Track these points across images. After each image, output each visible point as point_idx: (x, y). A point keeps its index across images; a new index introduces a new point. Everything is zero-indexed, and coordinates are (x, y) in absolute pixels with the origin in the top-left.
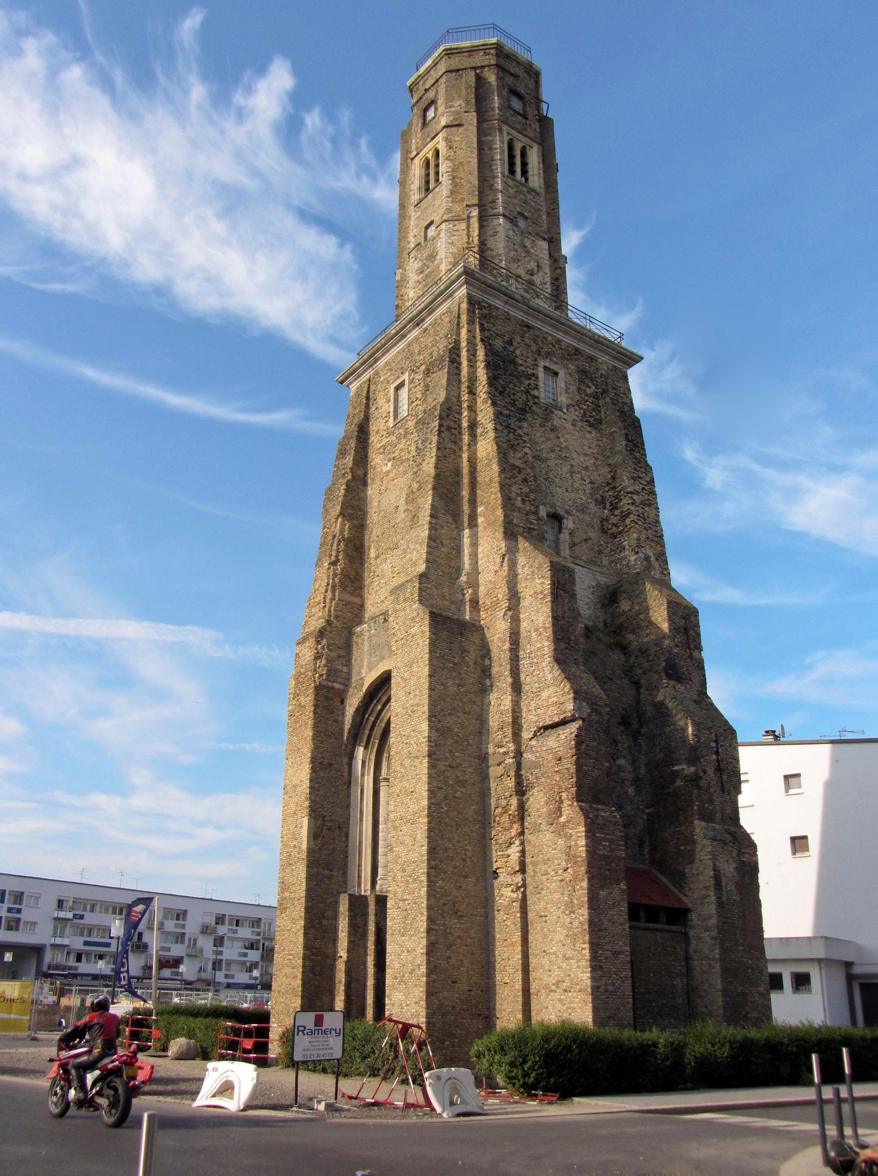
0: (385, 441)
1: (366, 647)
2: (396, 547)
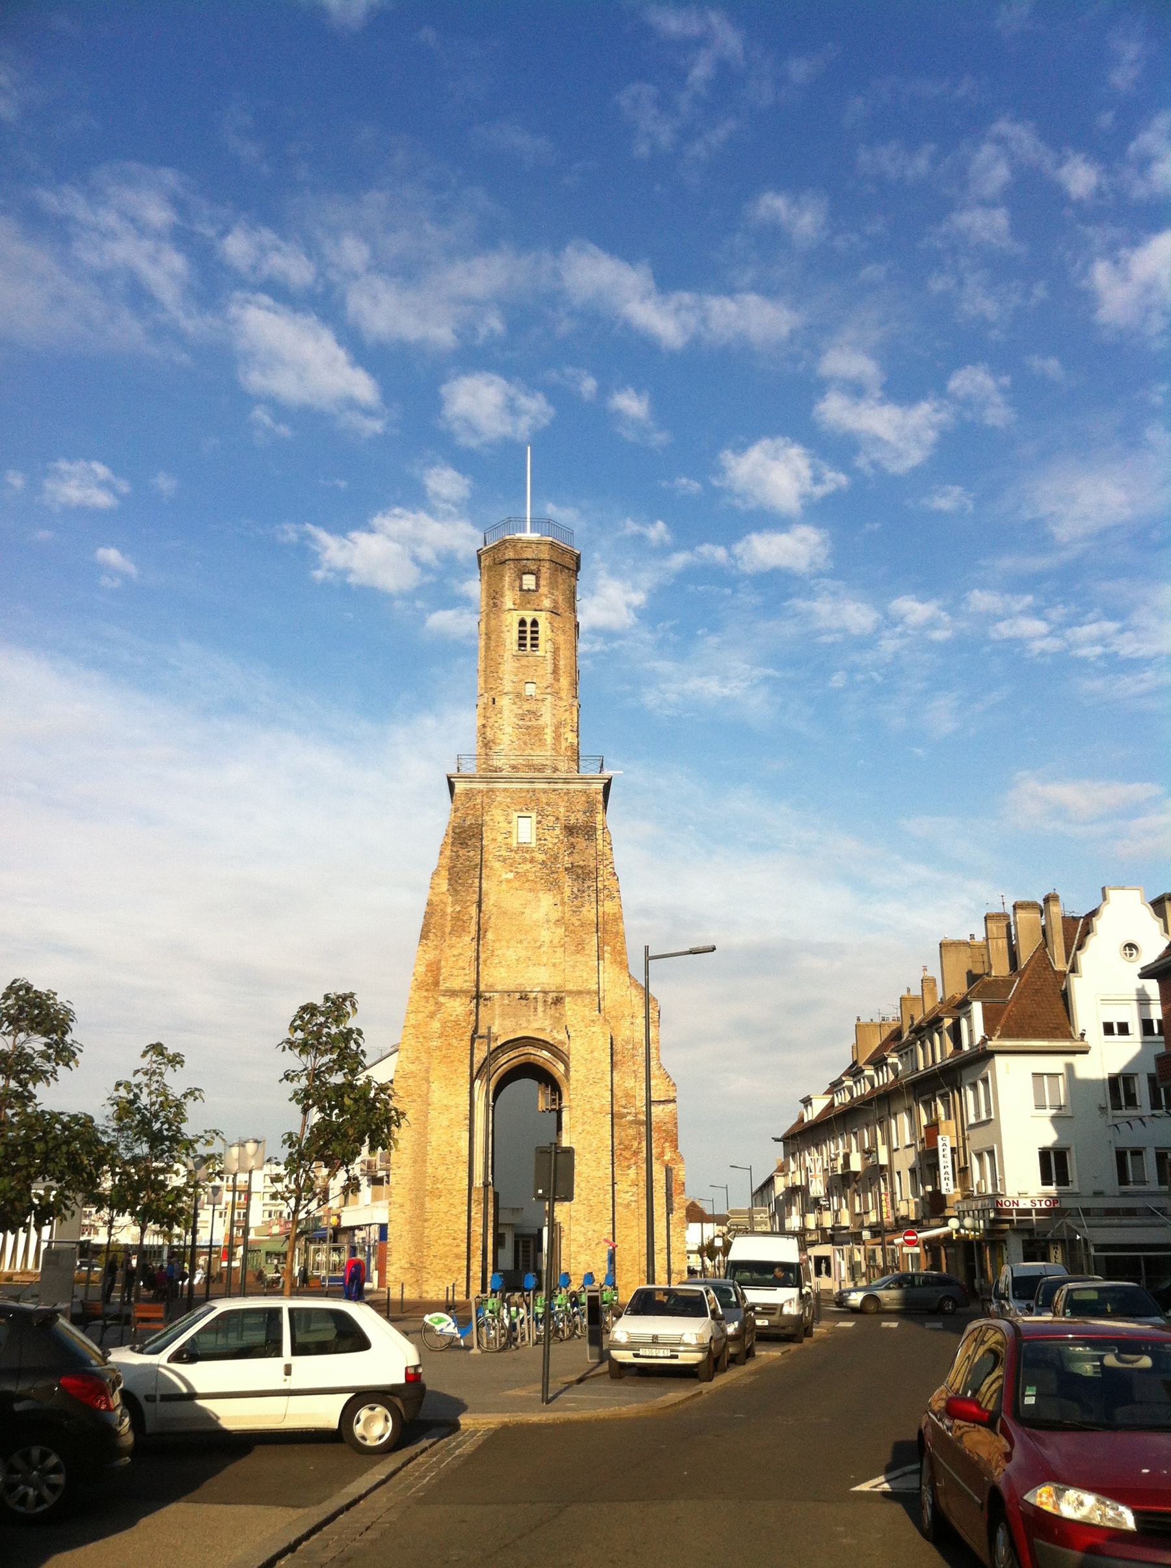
0: (503, 853)
1: (498, 1010)
2: (521, 942)
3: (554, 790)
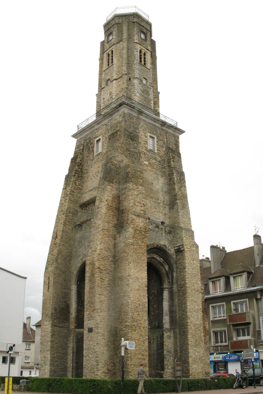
2: (152, 198)
3: (163, 129)
